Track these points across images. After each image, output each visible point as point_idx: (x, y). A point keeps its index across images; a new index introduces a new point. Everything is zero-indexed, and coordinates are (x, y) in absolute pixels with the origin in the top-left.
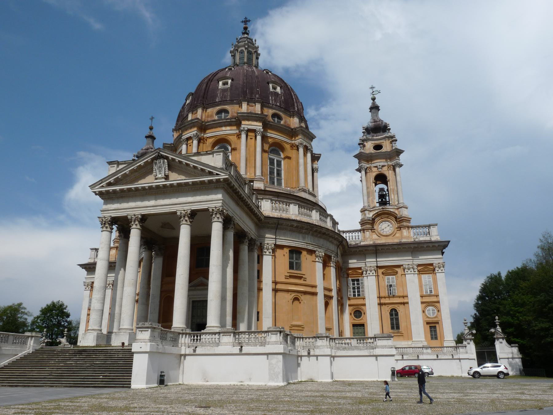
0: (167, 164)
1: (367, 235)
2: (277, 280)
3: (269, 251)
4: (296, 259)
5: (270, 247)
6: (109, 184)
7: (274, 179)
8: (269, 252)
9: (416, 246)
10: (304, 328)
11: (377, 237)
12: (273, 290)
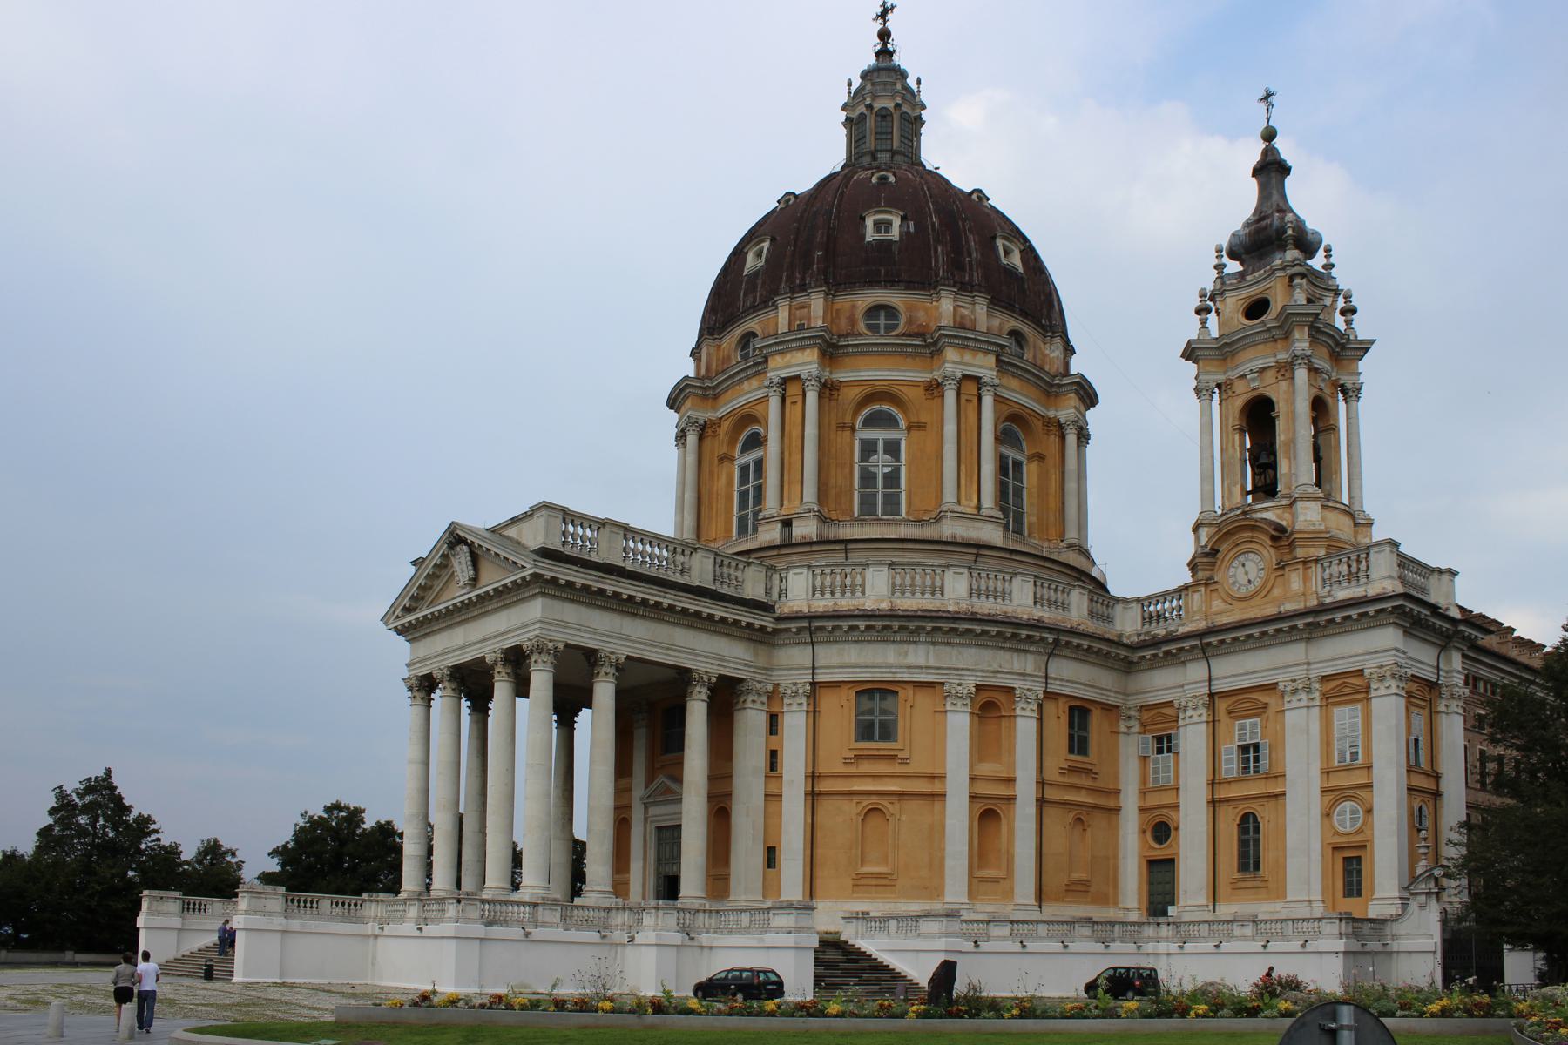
1: (1195, 603)
2: (821, 770)
3: (800, 701)
5: (801, 691)
9: (1310, 620)
11: (1224, 604)
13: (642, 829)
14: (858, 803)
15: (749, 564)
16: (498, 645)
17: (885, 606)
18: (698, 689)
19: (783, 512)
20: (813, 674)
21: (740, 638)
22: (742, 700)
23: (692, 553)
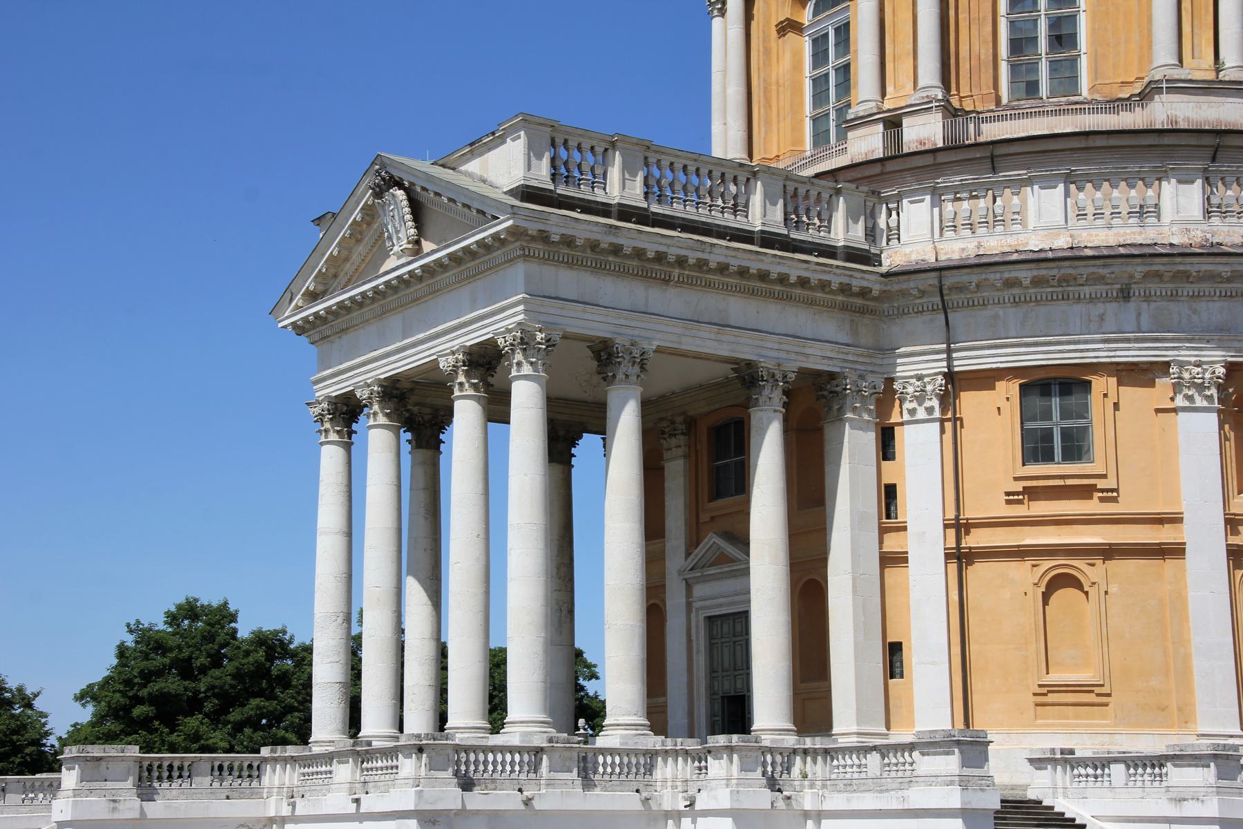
0: (405, 203)
2: (971, 512)
3: (928, 404)
4: (1065, 415)
5: (929, 388)
6: (313, 297)
7: (1033, 67)
8: (926, 409)
10: (1109, 695)
12: (948, 556)
13: (683, 620)
14: (1034, 566)
15: (838, 192)
16: (456, 342)
17: (1062, 242)
18: (766, 392)
19: (887, 105)
20: (949, 359)
21: (832, 306)
22: (836, 407)
23: (748, 180)
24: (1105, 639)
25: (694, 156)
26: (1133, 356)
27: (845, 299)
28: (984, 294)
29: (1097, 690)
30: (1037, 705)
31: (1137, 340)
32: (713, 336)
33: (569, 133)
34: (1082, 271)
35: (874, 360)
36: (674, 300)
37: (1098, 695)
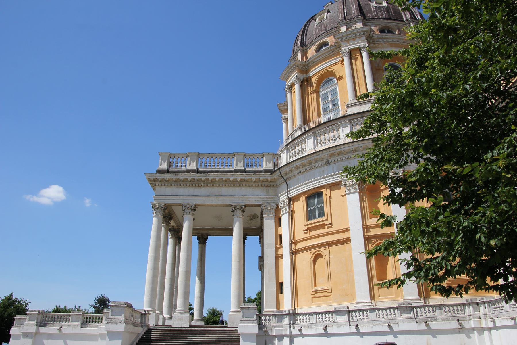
10: (331, 292)
12: (290, 253)
14: (311, 252)
21: (258, 186)
24: (329, 273)
25: (215, 154)
26: (332, 181)
27: (262, 183)
28: (294, 173)
29: (328, 291)
30: (313, 298)
31: (332, 176)
32: (215, 199)
33: (175, 155)
34: (312, 158)
35: (274, 199)
36: (203, 191)
37: (328, 293)
